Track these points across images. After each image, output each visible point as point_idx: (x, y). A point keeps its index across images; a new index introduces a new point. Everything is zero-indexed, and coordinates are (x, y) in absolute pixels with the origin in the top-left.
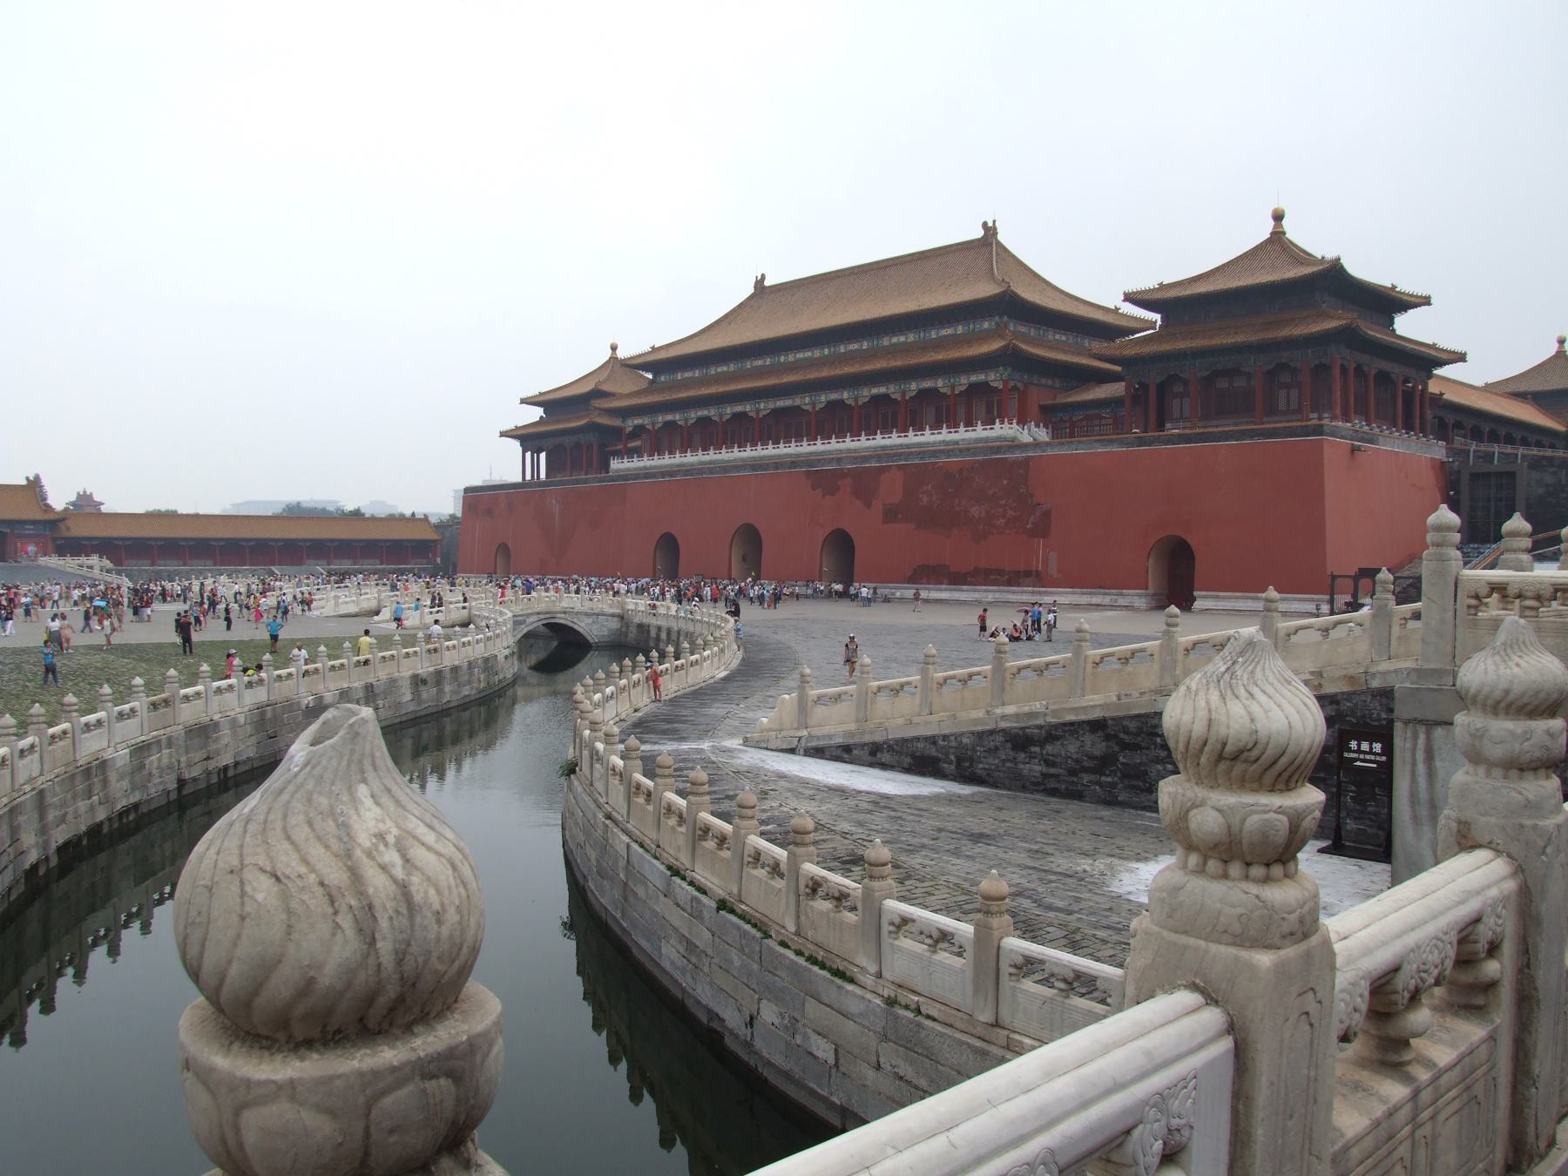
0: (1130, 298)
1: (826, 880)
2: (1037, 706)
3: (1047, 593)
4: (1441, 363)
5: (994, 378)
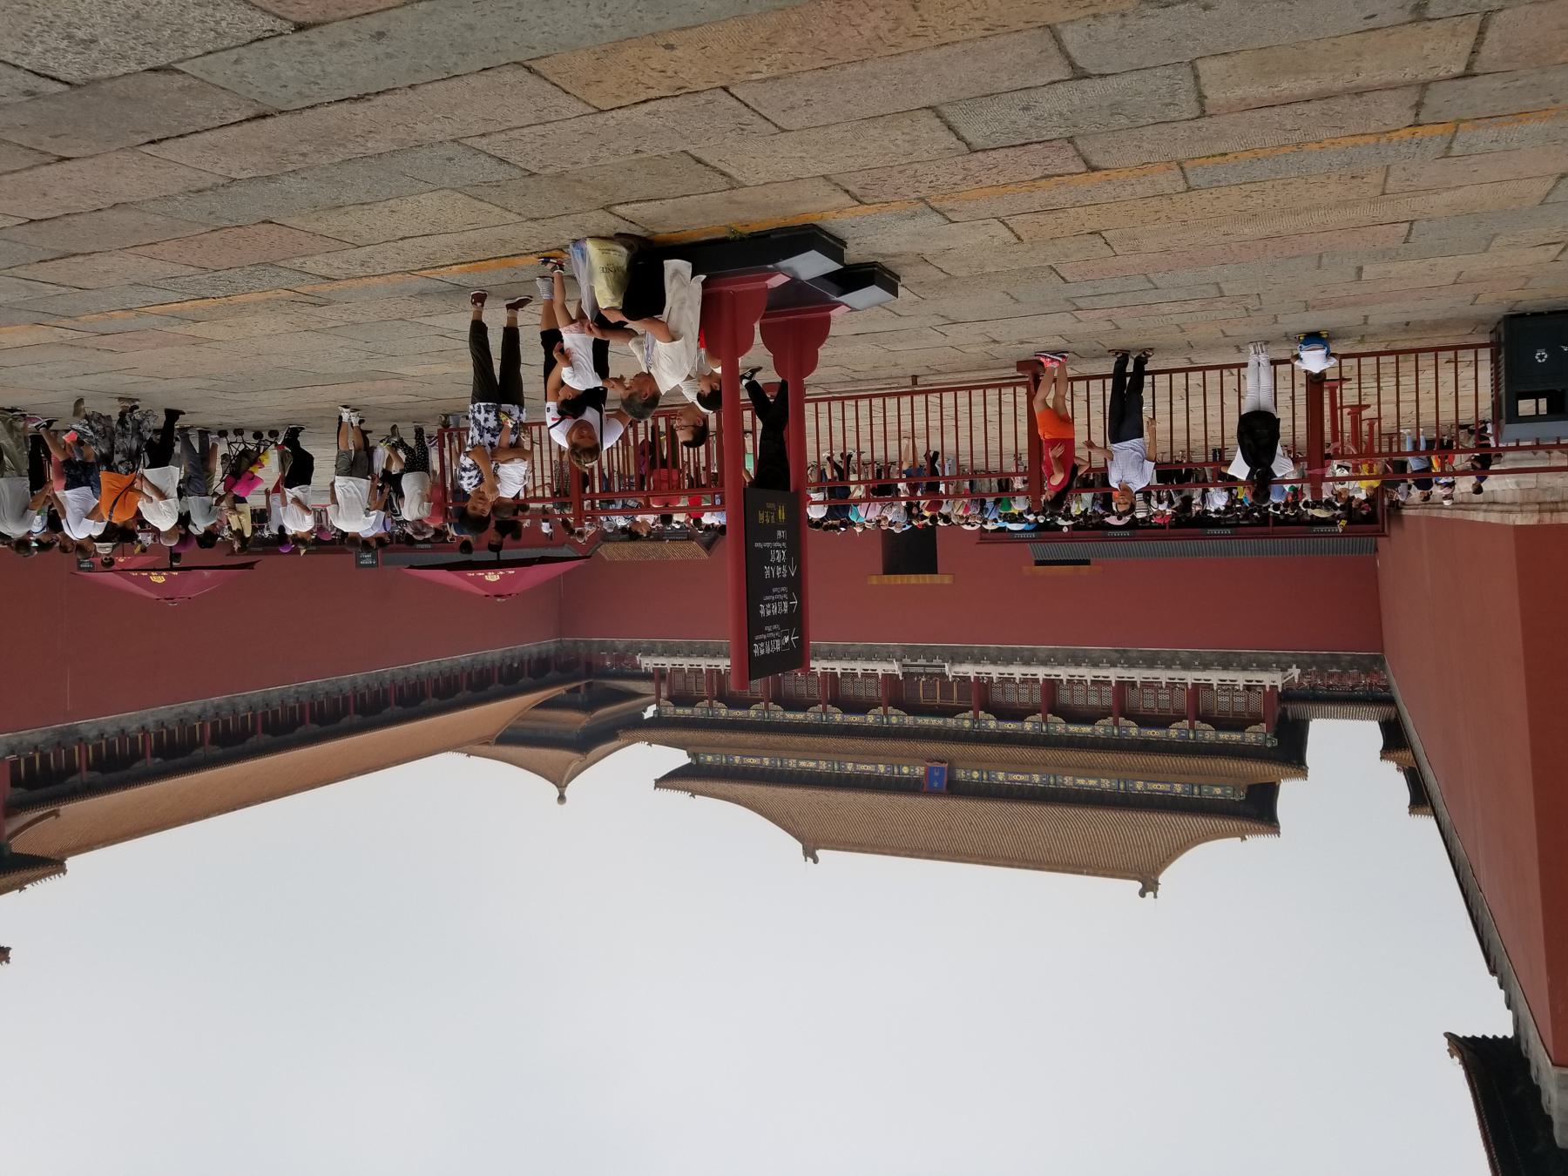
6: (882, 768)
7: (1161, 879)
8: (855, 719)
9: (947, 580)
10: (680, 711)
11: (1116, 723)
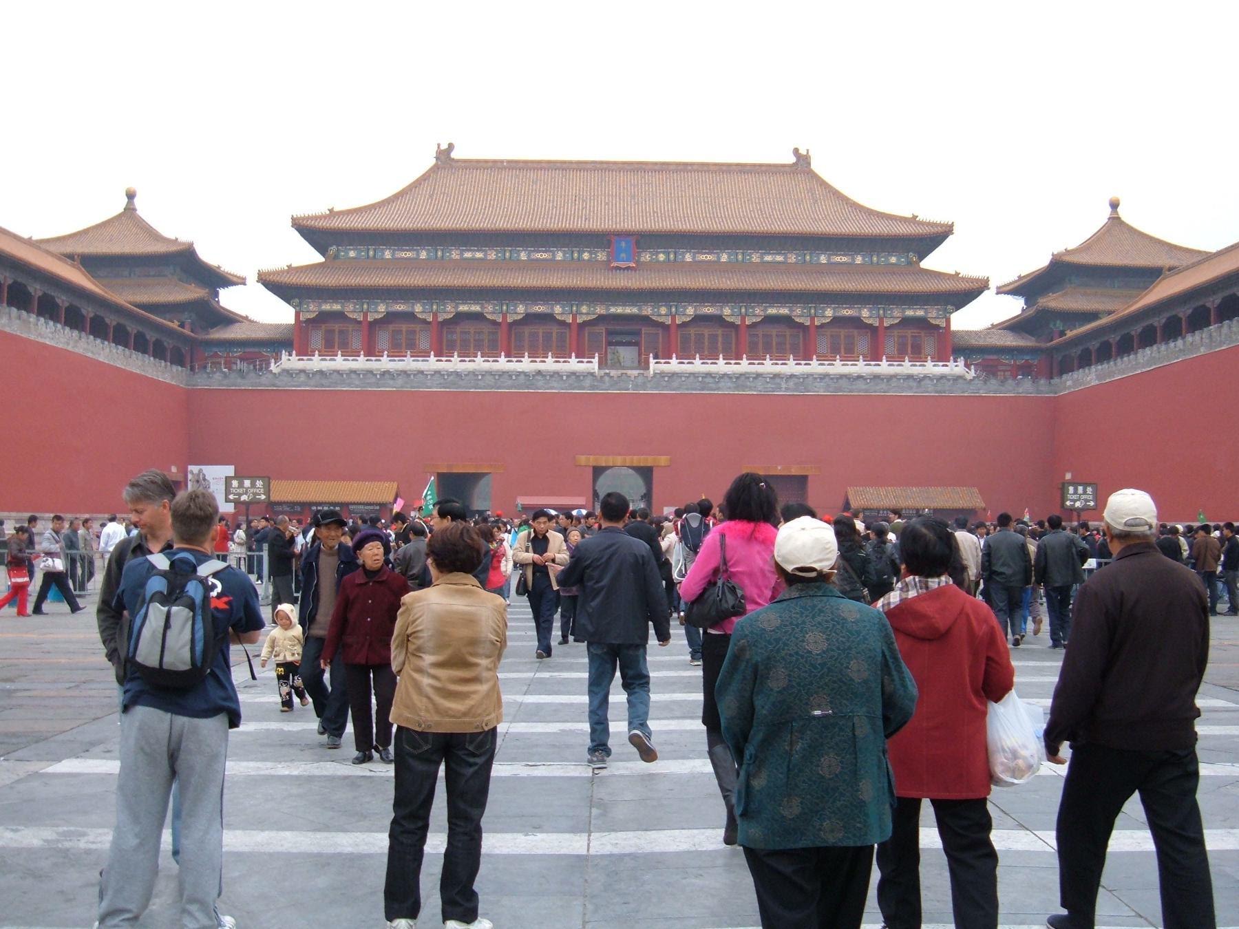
6: (688, 258)
7: (434, 161)
8: (708, 310)
9: (582, 459)
10: (920, 313)
11: (435, 315)
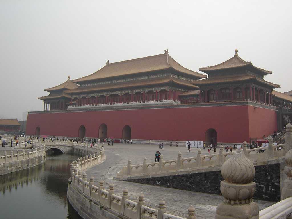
0: (201, 70)
1: (148, 209)
2: (189, 169)
3: (181, 142)
4: (275, 88)
5: (167, 88)
7: (106, 64)
